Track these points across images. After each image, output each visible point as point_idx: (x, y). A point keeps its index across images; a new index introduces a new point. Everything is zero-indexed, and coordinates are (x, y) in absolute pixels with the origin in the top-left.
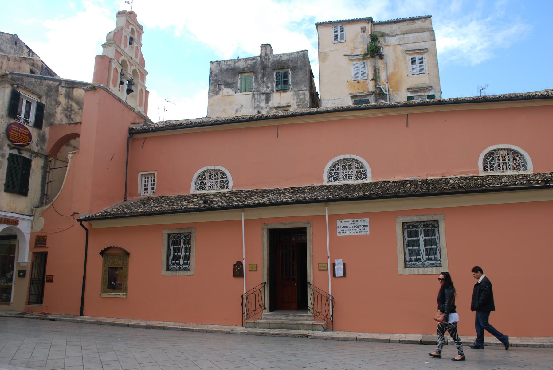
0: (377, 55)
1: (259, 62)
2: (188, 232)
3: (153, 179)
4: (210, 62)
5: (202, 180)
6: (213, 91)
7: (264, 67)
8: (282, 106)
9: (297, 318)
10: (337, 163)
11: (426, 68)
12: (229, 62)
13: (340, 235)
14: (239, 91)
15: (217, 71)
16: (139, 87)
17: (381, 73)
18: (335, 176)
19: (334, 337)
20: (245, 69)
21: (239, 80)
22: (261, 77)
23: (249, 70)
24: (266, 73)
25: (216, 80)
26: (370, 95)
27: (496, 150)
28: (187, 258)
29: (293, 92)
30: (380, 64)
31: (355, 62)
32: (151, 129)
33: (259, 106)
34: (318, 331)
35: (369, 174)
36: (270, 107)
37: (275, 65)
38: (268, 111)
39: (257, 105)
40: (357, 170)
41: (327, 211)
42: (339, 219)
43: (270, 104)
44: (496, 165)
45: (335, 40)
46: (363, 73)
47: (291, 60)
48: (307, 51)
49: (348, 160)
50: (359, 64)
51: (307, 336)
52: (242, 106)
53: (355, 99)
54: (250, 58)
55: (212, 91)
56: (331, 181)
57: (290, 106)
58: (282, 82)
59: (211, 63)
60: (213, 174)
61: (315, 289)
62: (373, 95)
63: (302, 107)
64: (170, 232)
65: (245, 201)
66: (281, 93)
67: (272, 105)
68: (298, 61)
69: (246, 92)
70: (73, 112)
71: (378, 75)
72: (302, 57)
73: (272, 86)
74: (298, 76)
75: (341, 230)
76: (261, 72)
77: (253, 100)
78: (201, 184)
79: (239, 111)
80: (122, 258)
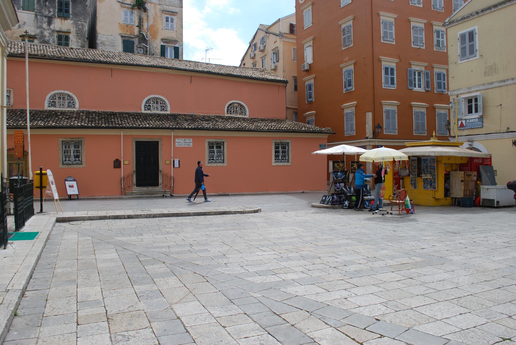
0: (142, 8)
2: (79, 140)
11: (175, 27)
14: (21, 8)
17: (144, 22)
26: (136, 38)
27: (234, 103)
29: (73, 21)
30: (144, 15)
31: (125, 9)
33: (40, 27)
35: (169, 108)
36: (51, 29)
40: (161, 105)
41: (172, 134)
42: (177, 138)
43: (52, 27)
44: (232, 111)
46: (131, 20)
49: (157, 98)
50: (129, 12)
53: (124, 39)
57: (70, 33)
58: (64, 10)
60: (61, 97)
61: (164, 173)
62: (137, 38)
71: (142, 23)
73: (54, 11)
74: (77, 8)
79: (22, 27)
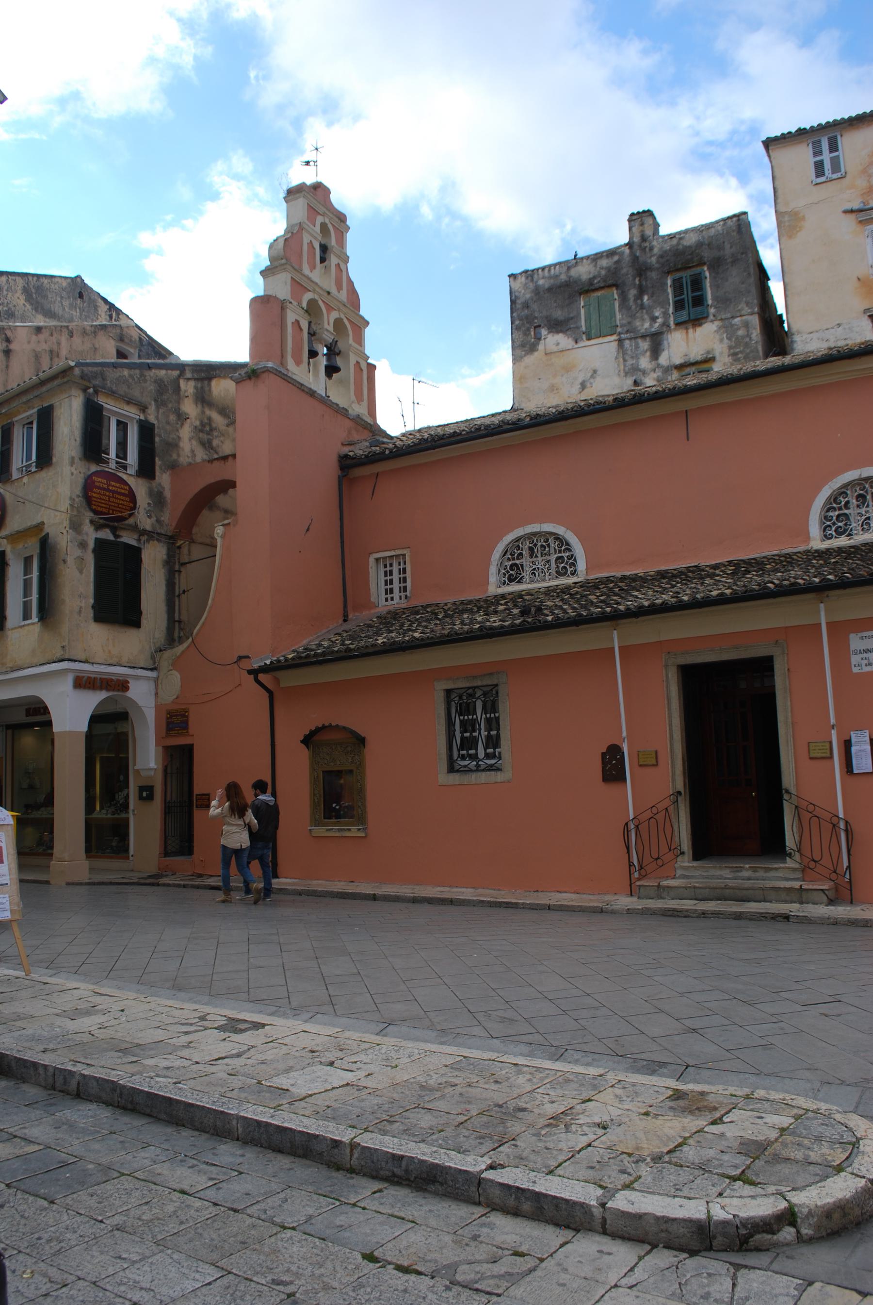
1: (627, 259)
2: (489, 683)
3: (401, 567)
4: (510, 276)
5: (514, 559)
6: (523, 345)
7: (641, 270)
8: (692, 360)
9: (761, 874)
10: (842, 492)
12: (555, 268)
13: (861, 671)
14: (584, 337)
15: (528, 296)
16: (353, 359)
18: (840, 524)
19: (856, 920)
20: (596, 281)
21: (582, 311)
22: (635, 296)
23: (605, 281)
24: (648, 282)
25: (527, 317)
28: (493, 742)
32: (387, 452)
33: (635, 369)
34: (814, 903)
36: (662, 367)
37: (668, 260)
38: (658, 376)
39: (630, 367)
43: (663, 360)
45: (817, 176)
47: (706, 242)
48: (745, 213)
51: (787, 918)
52: (595, 372)
54: (603, 252)
55: (519, 346)
56: (830, 537)
59: (512, 279)
61: (804, 804)
63: (744, 358)
64: (450, 685)
65: (618, 603)
66: (687, 329)
67: (668, 361)
68: (726, 243)
69: (600, 336)
70: (215, 433)
72: (733, 231)
73: (665, 314)
74: (727, 280)
75: (862, 659)
76: (635, 284)
77: (621, 355)
78: (512, 570)
79: (588, 385)
80: (349, 749)
